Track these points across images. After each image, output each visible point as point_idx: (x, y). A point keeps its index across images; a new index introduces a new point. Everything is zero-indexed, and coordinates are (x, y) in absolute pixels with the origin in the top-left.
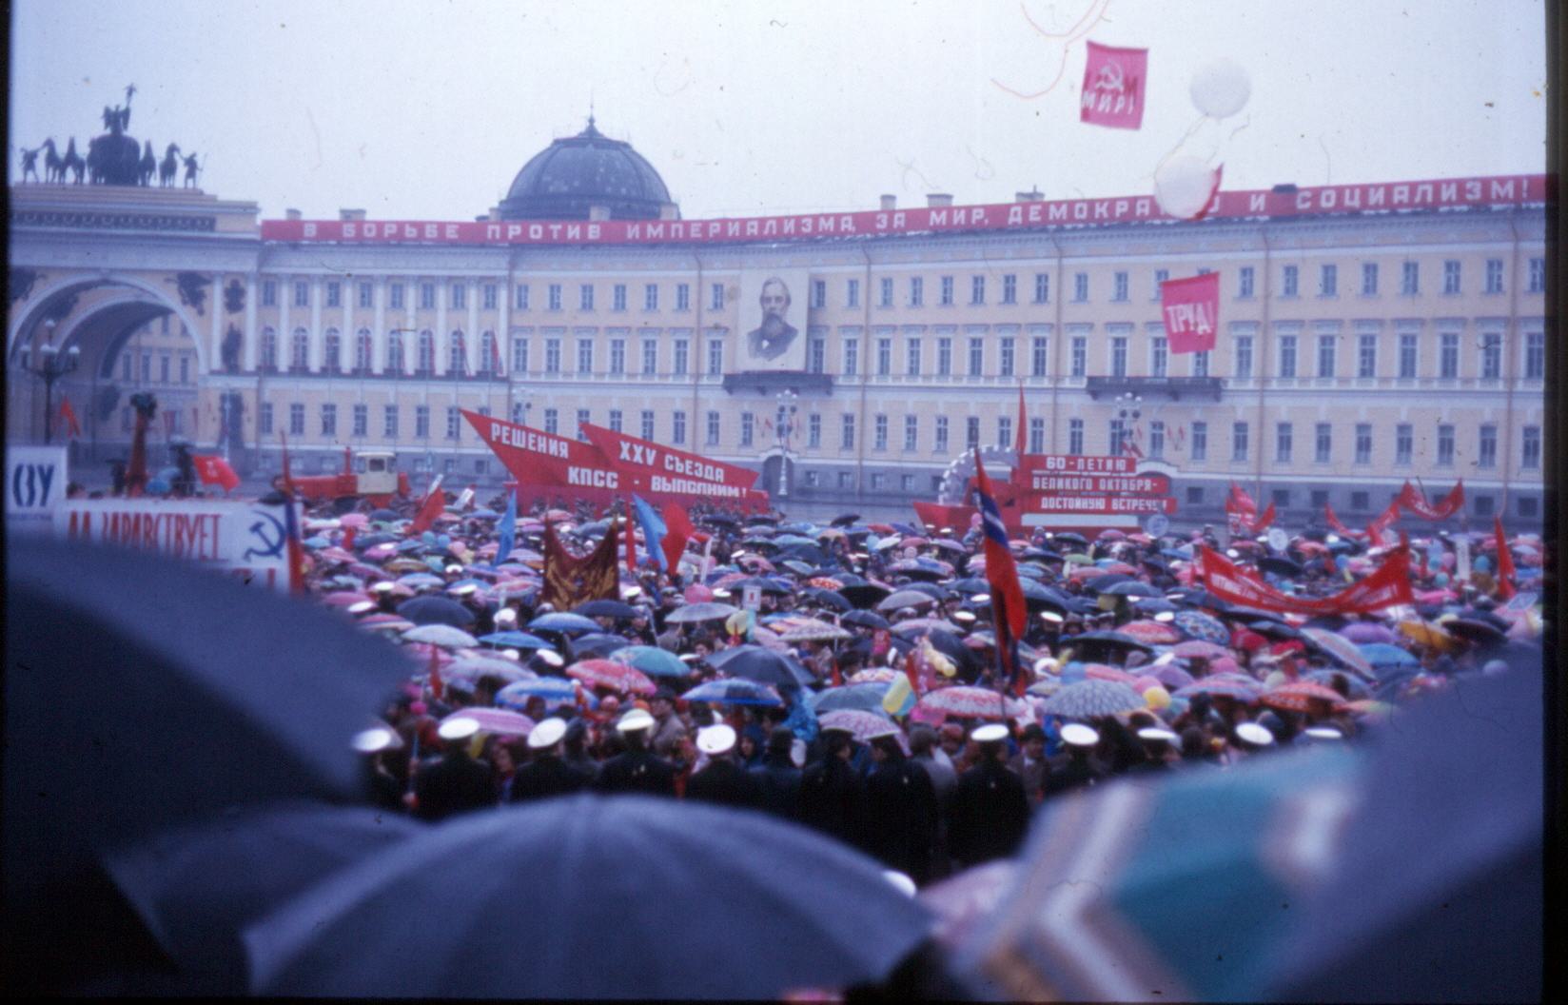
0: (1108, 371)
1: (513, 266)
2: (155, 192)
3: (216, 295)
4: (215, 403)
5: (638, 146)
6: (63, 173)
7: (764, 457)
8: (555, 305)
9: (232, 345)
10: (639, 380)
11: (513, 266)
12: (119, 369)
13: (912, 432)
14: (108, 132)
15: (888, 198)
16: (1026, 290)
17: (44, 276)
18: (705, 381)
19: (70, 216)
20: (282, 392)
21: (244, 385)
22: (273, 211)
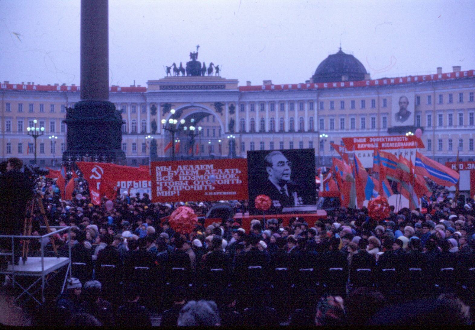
1: (318, 96)
2: (207, 78)
3: (226, 109)
5: (357, 56)
6: (178, 74)
8: (332, 108)
9: (232, 124)
10: (360, 131)
11: (318, 96)
13: (451, 144)
14: (192, 60)
15: (439, 69)
17: (174, 105)
18: (382, 130)
19: (181, 86)
22: (242, 83)
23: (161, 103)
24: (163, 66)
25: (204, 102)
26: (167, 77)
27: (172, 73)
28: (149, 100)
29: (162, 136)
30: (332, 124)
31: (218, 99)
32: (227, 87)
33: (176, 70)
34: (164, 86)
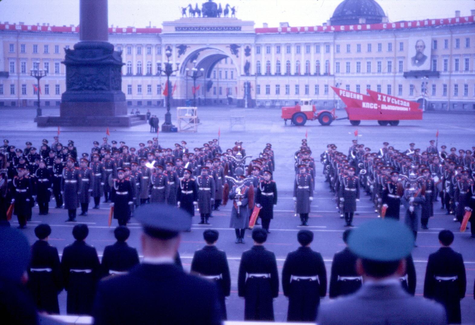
1: (335, 39)
4: (242, 84)
6: (194, 15)
7: (417, 99)
8: (348, 51)
9: (247, 67)
10: (376, 75)
11: (335, 39)
12: (212, 75)
13: (466, 90)
15: (457, 12)
17: (189, 47)
18: (397, 74)
19: (197, 28)
20: (263, 81)
22: (259, 25)
24: (179, 7)
25: (219, 44)
26: (183, 18)
27: (188, 14)
28: (165, 41)
29: (177, 77)
30: (348, 67)
31: (234, 41)
32: (242, 29)
33: (192, 12)
34: (179, 28)
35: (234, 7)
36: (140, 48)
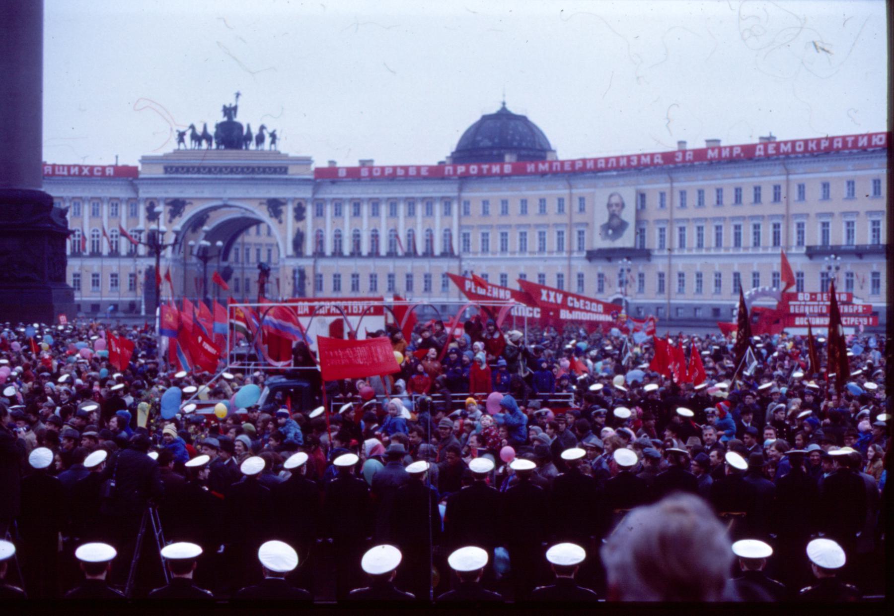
0: (819, 242)
1: (460, 190)
2: (253, 152)
3: (289, 212)
4: (289, 273)
5: (533, 118)
6: (200, 144)
8: (486, 212)
9: (299, 241)
11: (460, 190)
12: (232, 256)
13: (699, 282)
14: (225, 119)
16: (767, 194)
17: (191, 203)
18: (575, 255)
20: (328, 267)
21: (306, 264)
22: (321, 162)
23: (166, 199)
25: (247, 199)
26: (179, 149)
27: (189, 144)
28: (145, 193)
34: (171, 168)
35: (274, 131)
36: (98, 205)
